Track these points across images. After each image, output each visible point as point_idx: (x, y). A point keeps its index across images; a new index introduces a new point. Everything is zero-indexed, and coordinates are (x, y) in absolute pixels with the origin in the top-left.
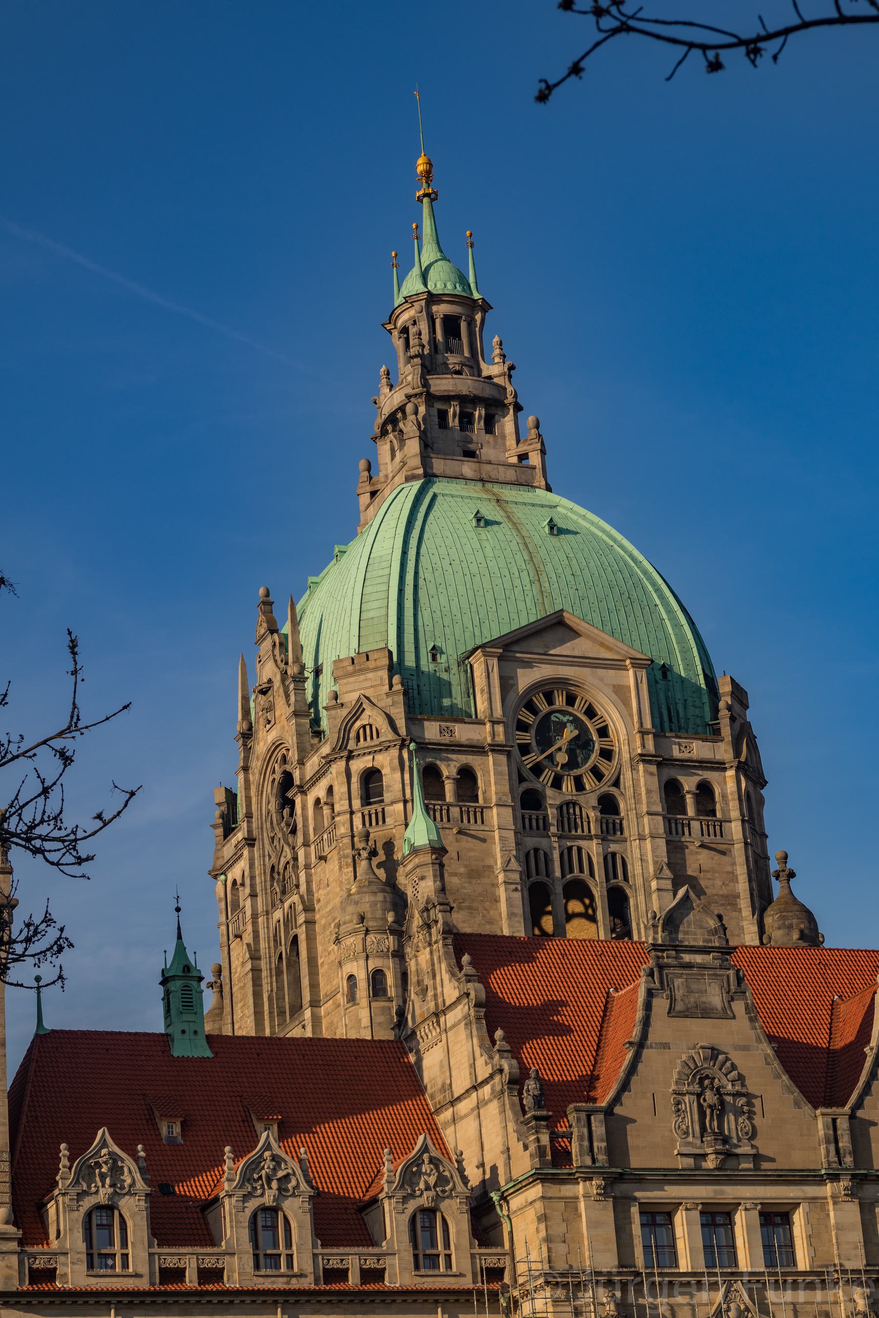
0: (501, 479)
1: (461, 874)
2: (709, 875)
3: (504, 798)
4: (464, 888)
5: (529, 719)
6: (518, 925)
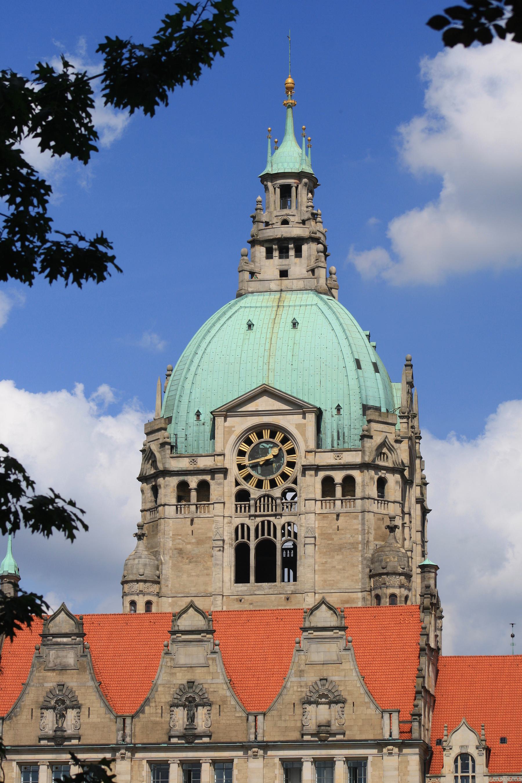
0: (294, 288)
2: (343, 532)
4: (194, 550)
5: (245, 448)
6: (219, 570)
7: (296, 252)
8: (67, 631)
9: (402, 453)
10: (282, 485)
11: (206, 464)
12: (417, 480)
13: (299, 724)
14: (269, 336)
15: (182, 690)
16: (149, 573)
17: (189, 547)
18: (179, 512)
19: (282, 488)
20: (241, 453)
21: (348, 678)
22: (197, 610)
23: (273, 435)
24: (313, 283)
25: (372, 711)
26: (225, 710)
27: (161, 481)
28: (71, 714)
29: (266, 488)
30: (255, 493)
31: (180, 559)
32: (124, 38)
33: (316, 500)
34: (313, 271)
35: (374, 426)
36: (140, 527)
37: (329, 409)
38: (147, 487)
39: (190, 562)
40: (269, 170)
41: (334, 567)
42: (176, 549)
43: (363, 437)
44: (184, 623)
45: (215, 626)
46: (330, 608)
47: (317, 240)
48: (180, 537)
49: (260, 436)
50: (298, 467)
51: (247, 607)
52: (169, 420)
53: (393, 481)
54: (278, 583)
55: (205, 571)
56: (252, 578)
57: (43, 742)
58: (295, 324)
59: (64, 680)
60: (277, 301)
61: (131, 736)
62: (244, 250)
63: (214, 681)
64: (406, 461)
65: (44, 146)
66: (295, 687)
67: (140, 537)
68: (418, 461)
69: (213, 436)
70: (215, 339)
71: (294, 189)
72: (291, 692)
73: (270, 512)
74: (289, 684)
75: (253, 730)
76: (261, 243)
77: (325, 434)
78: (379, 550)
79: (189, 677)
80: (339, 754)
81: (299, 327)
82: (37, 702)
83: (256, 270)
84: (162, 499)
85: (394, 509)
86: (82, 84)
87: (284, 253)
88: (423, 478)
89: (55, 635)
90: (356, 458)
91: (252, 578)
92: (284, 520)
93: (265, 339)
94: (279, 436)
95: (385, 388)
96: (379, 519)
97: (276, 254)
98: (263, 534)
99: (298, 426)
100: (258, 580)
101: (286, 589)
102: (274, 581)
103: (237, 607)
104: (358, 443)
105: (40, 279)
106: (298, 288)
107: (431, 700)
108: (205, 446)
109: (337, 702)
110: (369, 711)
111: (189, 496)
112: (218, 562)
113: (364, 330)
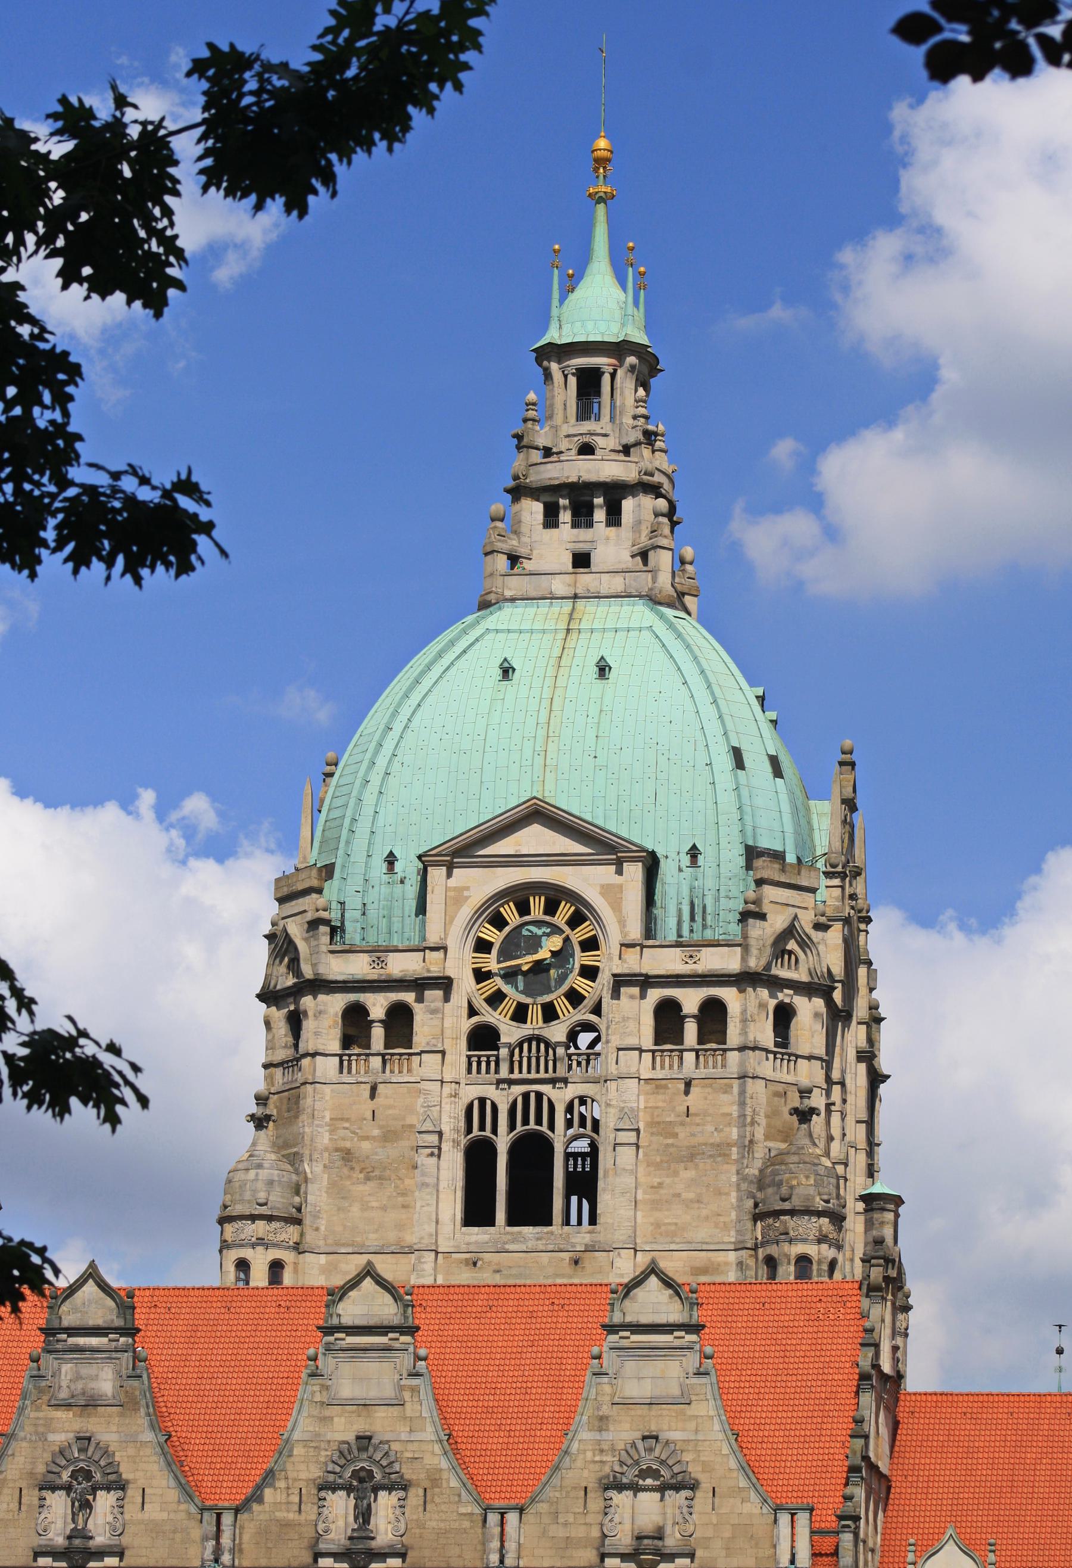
0: (604, 591)
1: (374, 1137)
2: (697, 1120)
3: (434, 1041)
4: (376, 1154)
6: (428, 1197)
7: (608, 514)
8: (100, 1322)
9: (830, 952)
10: (570, 1016)
11: (405, 967)
12: (861, 1010)
13: (595, 1533)
14: (547, 694)
15: (344, 1453)
16: (279, 1200)
17: (366, 1146)
18: (345, 1070)
19: (568, 1023)
20: (483, 946)
21: (702, 1435)
22: (381, 1283)
23: (551, 908)
24: (644, 581)
25: (753, 1507)
26: (437, 1500)
27: (307, 1002)
28: (104, 1501)
29: (535, 1024)
30: (510, 1033)
31: (345, 1171)
32: (246, 47)
33: (641, 1051)
34: (644, 555)
35: (770, 892)
36: (261, 1100)
37: (673, 855)
38: (279, 1015)
39: (368, 1179)
40: (554, 335)
41: (679, 1195)
42: (337, 1150)
43: (745, 916)
44: (351, 1311)
45: (419, 1318)
46: (668, 1283)
47: (655, 490)
48: (347, 1125)
49: (523, 909)
50: (604, 979)
51: (487, 1277)
52: (328, 871)
53: (808, 1011)
54: (556, 1227)
55: (400, 1199)
56: (501, 1215)
57: (42, 1561)
58: (603, 670)
59: (90, 1427)
60: (566, 618)
61: (232, 1551)
62: (497, 508)
63: (415, 1437)
64: (838, 970)
65: (68, 276)
66: (587, 1454)
67: (260, 1122)
68: (862, 971)
69: (421, 908)
70: (430, 699)
71: (606, 379)
72: (579, 1463)
73: (542, 1075)
74: (575, 1446)
75: (495, 1544)
76: (534, 492)
77: (664, 908)
78: (774, 1160)
79: (361, 1426)
81: (613, 675)
82: (31, 1474)
83: (523, 551)
84: (308, 1043)
85: (809, 1073)
86: (155, 146)
87: (582, 516)
88: (874, 1007)
89: (73, 1331)
90: (729, 961)
91: (501, 1215)
92: (571, 1091)
93: (537, 699)
94: (565, 911)
95: (795, 811)
96: (776, 1094)
97: (565, 516)
98: (526, 1122)
99: (606, 890)
100: (513, 1220)
101: (573, 1241)
102: (549, 1222)
103: (466, 1276)
104: (735, 929)
105: (53, 564)
106: (612, 591)
107: (881, 1486)
108: (406, 930)
109: (677, 1488)
110: (747, 1508)
111: (368, 1037)
112: (427, 1180)
113: (752, 684)
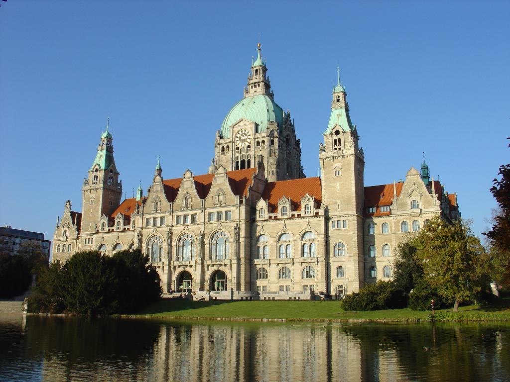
10: (247, 144)
49: (242, 132)
80: (224, 210)
87: (255, 86)
97: (254, 87)
